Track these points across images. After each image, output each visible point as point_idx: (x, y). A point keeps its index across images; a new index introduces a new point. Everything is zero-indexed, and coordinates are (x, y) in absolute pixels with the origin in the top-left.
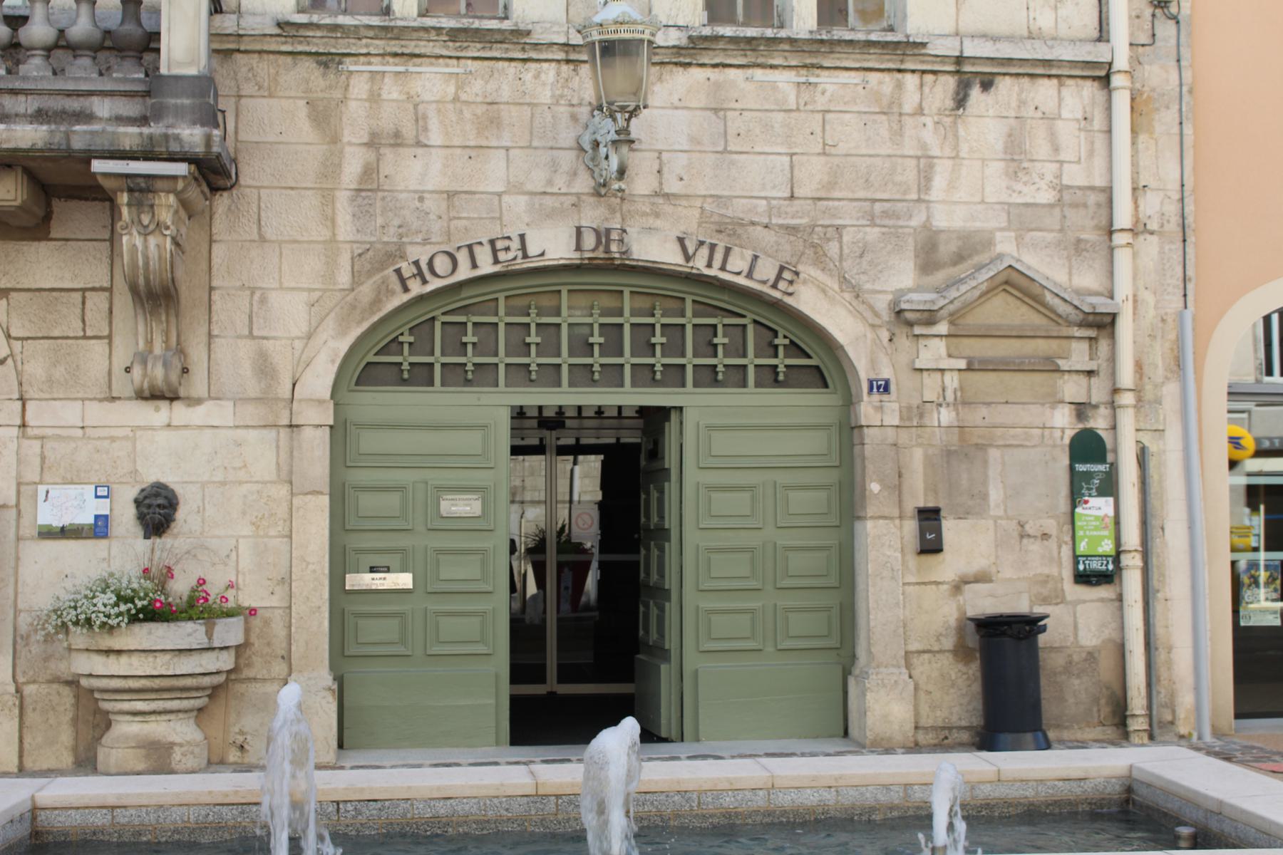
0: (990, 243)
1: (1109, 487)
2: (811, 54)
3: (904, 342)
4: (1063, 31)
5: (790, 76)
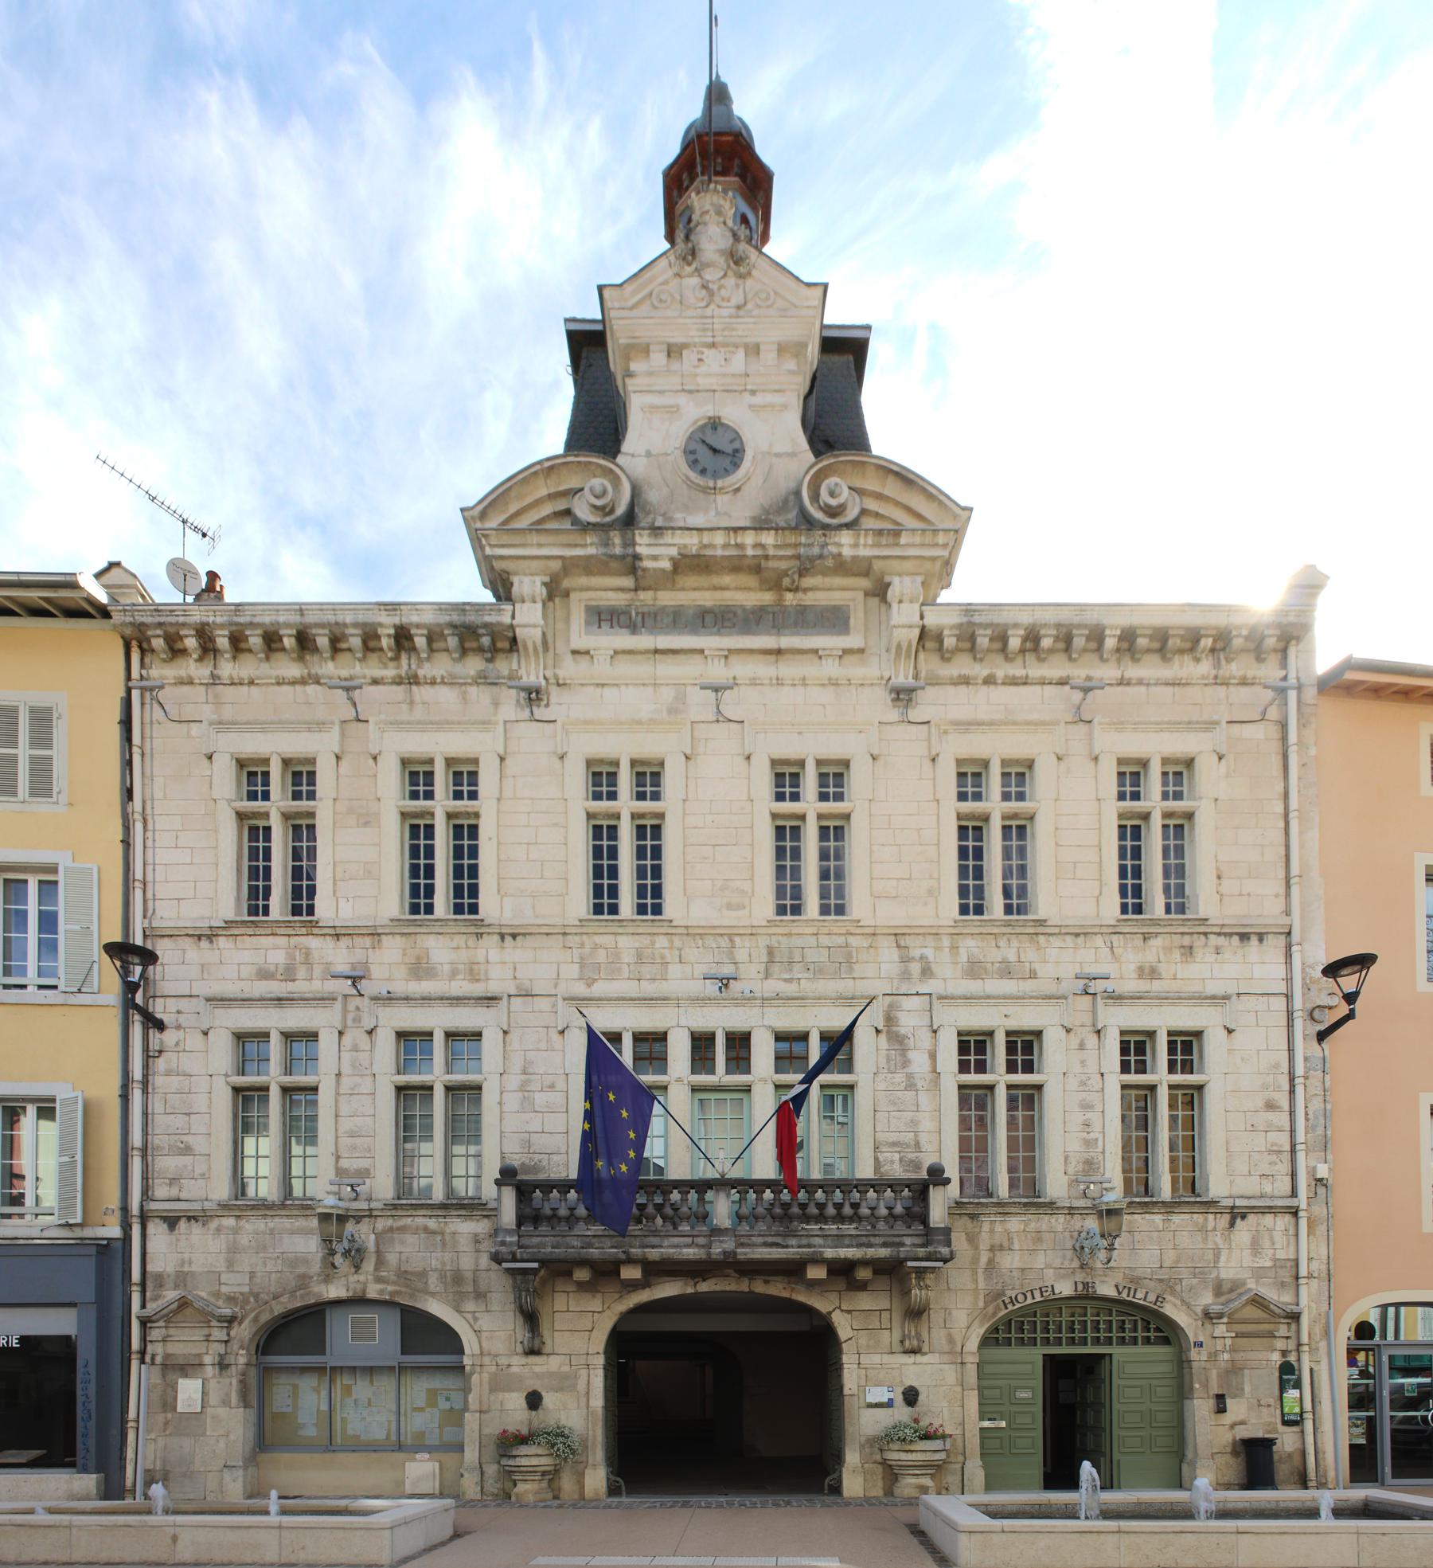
0: (1244, 1284)
1: (1298, 1385)
2: (1170, 1207)
3: (1208, 1326)
4: (1276, 1193)
5: (1160, 1217)
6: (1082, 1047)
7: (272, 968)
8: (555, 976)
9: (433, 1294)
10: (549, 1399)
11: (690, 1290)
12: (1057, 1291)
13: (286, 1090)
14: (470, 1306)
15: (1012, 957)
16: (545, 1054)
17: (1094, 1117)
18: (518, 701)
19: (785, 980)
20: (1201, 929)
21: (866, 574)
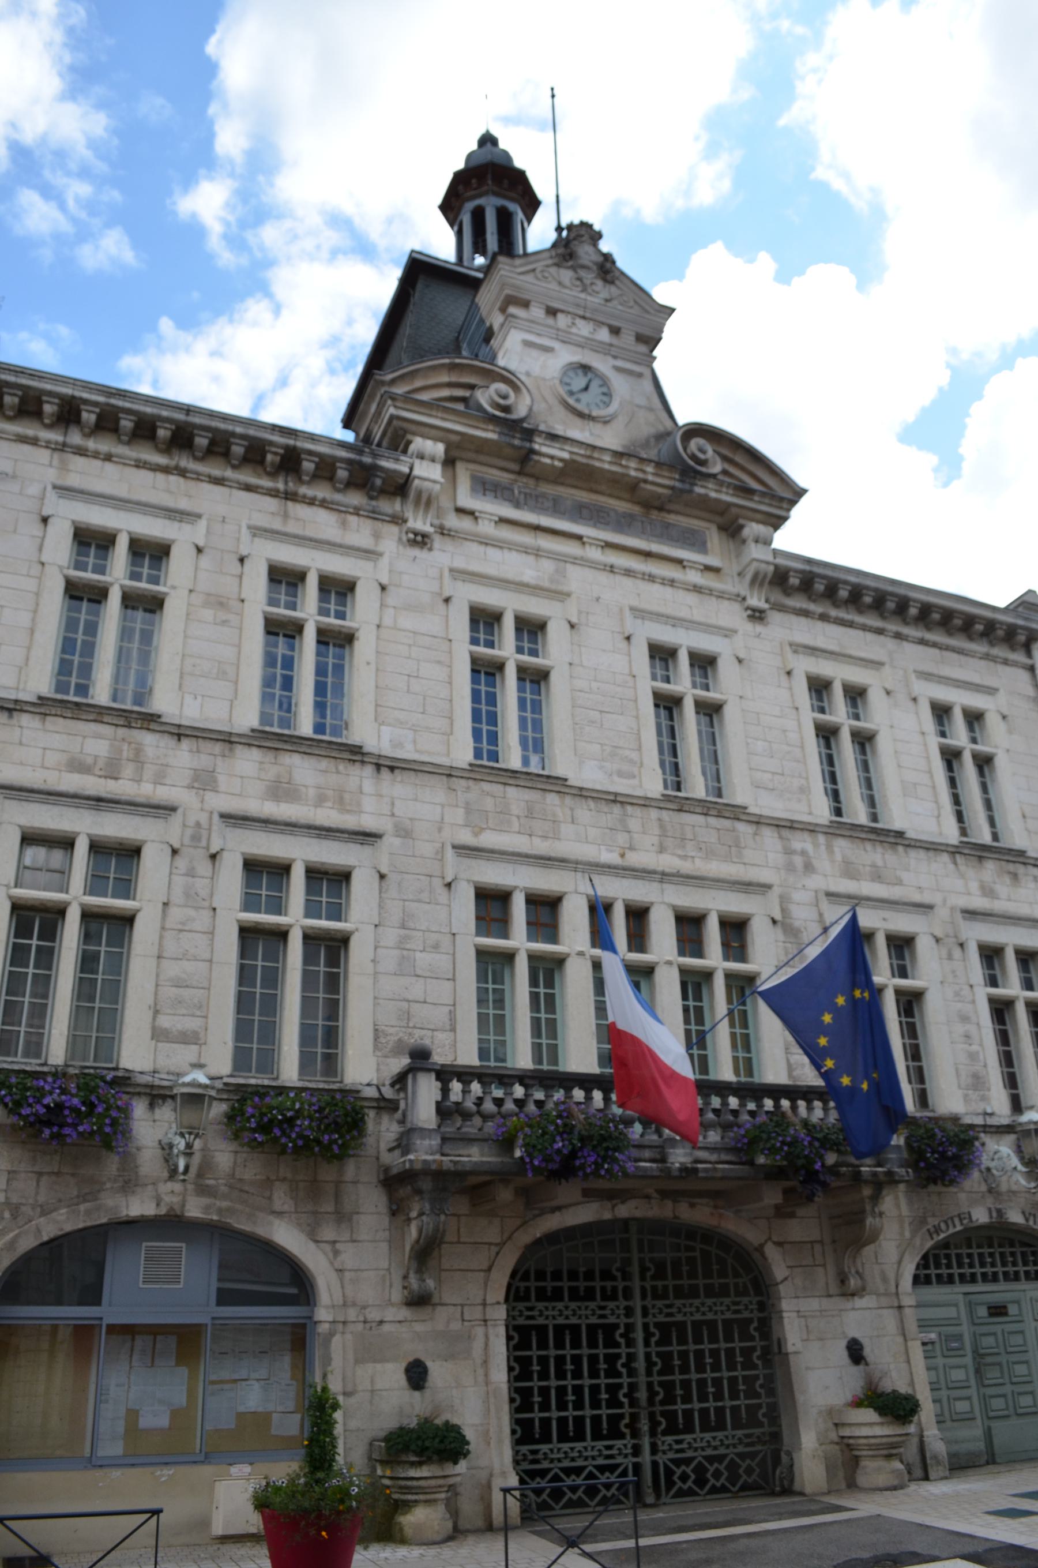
6: (950, 957)
7: (90, 760)
8: (438, 818)
9: (279, 1214)
10: (438, 1372)
11: (607, 1216)
12: (974, 1218)
13: (88, 916)
14: (328, 1233)
15: (880, 863)
16: (427, 907)
17: (972, 1029)
18: (400, 539)
19: (680, 856)
20: (1021, 860)
21: (722, 514)
